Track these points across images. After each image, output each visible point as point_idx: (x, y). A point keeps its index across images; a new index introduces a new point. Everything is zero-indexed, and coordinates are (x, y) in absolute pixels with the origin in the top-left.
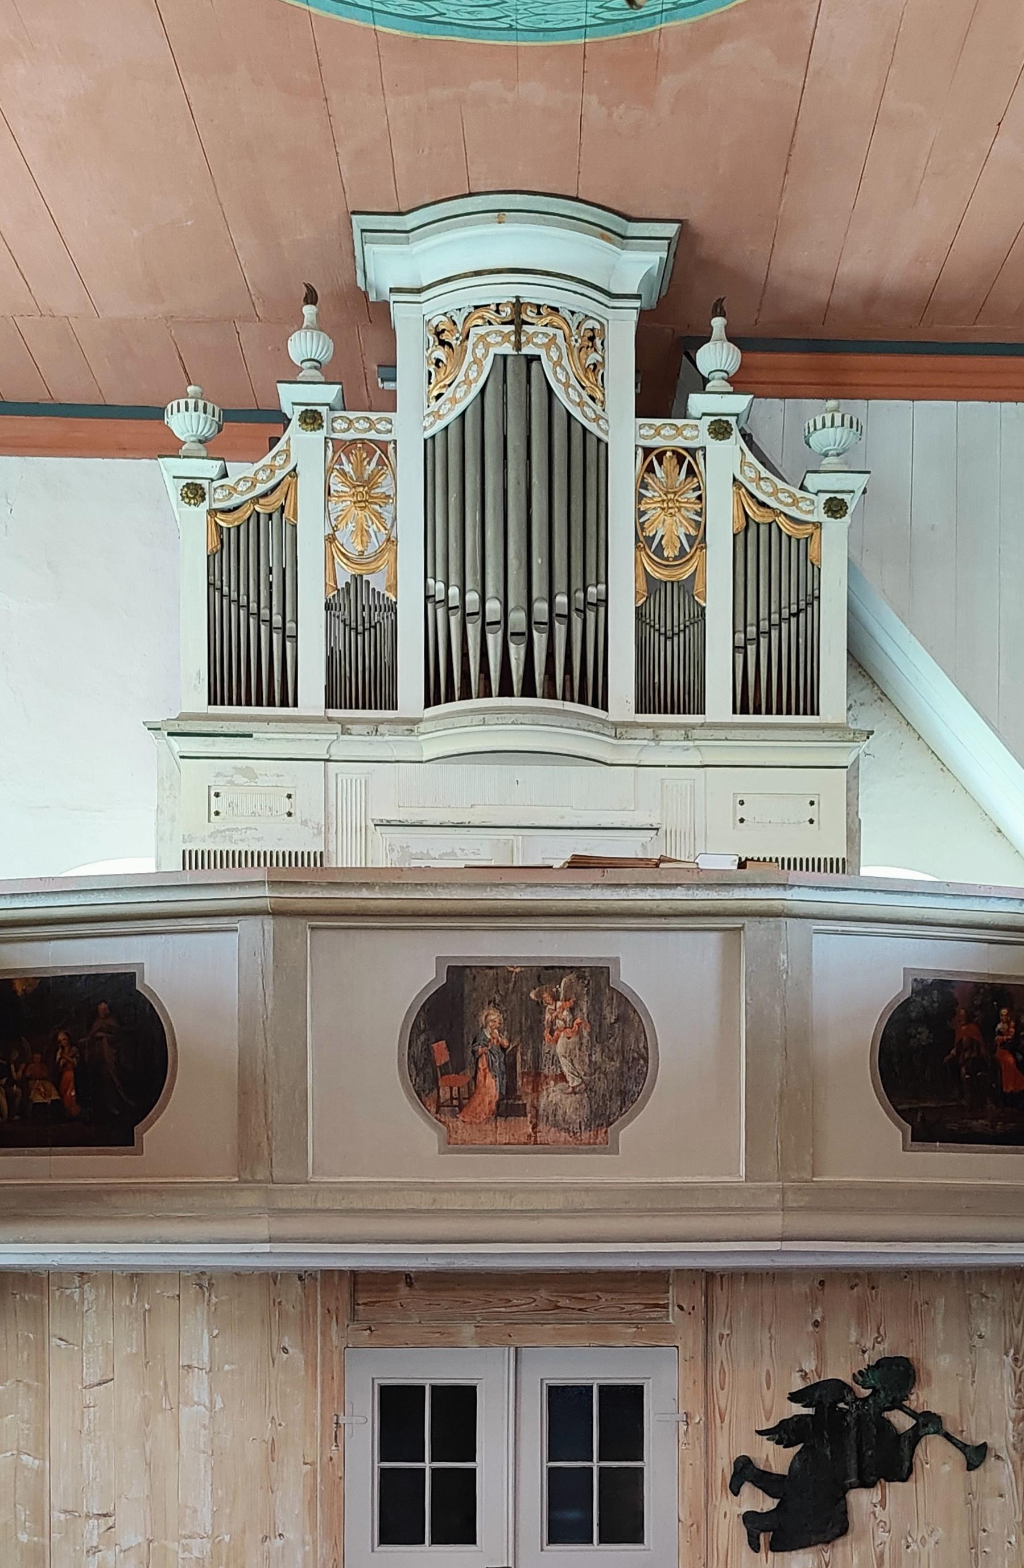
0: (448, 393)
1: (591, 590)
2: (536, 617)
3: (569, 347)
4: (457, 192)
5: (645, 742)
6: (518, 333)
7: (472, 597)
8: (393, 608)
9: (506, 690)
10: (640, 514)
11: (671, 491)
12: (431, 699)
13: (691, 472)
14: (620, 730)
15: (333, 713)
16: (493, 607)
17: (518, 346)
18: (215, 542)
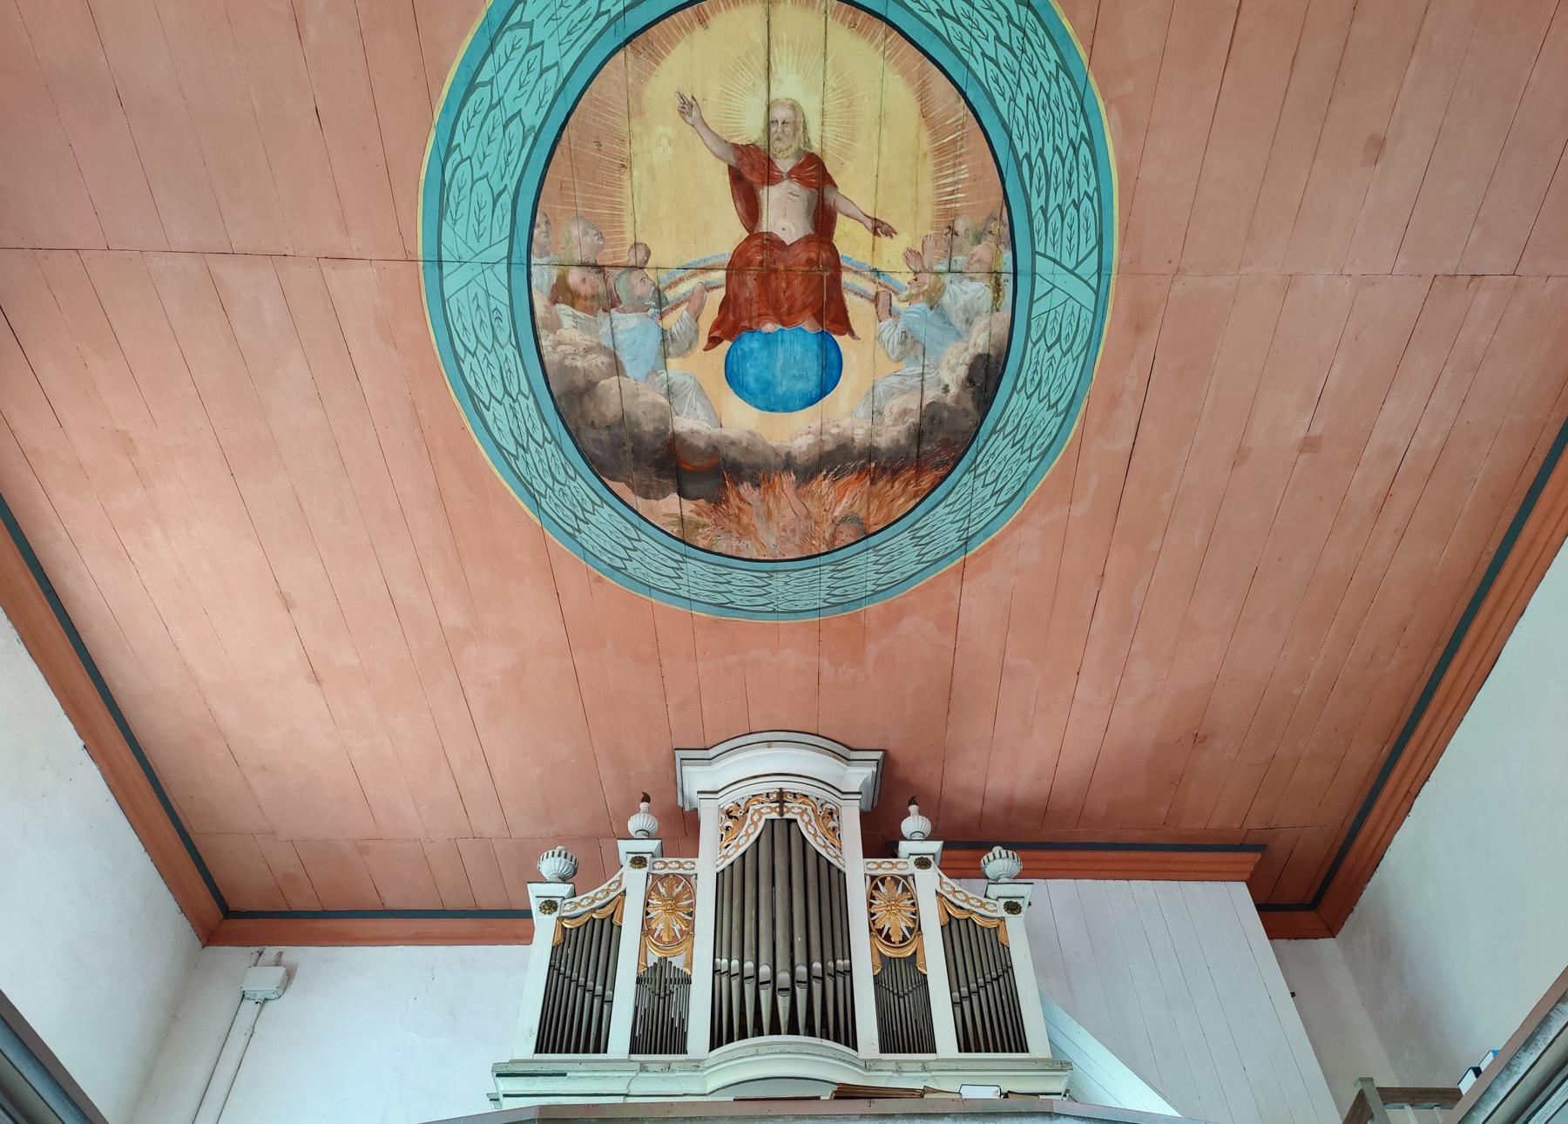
1: (839, 962)
2: (798, 978)
3: (817, 817)
6: (781, 807)
7: (749, 965)
9: (775, 1030)
10: (872, 915)
12: (715, 1043)
15: (634, 1057)
16: (765, 970)
17: (781, 814)
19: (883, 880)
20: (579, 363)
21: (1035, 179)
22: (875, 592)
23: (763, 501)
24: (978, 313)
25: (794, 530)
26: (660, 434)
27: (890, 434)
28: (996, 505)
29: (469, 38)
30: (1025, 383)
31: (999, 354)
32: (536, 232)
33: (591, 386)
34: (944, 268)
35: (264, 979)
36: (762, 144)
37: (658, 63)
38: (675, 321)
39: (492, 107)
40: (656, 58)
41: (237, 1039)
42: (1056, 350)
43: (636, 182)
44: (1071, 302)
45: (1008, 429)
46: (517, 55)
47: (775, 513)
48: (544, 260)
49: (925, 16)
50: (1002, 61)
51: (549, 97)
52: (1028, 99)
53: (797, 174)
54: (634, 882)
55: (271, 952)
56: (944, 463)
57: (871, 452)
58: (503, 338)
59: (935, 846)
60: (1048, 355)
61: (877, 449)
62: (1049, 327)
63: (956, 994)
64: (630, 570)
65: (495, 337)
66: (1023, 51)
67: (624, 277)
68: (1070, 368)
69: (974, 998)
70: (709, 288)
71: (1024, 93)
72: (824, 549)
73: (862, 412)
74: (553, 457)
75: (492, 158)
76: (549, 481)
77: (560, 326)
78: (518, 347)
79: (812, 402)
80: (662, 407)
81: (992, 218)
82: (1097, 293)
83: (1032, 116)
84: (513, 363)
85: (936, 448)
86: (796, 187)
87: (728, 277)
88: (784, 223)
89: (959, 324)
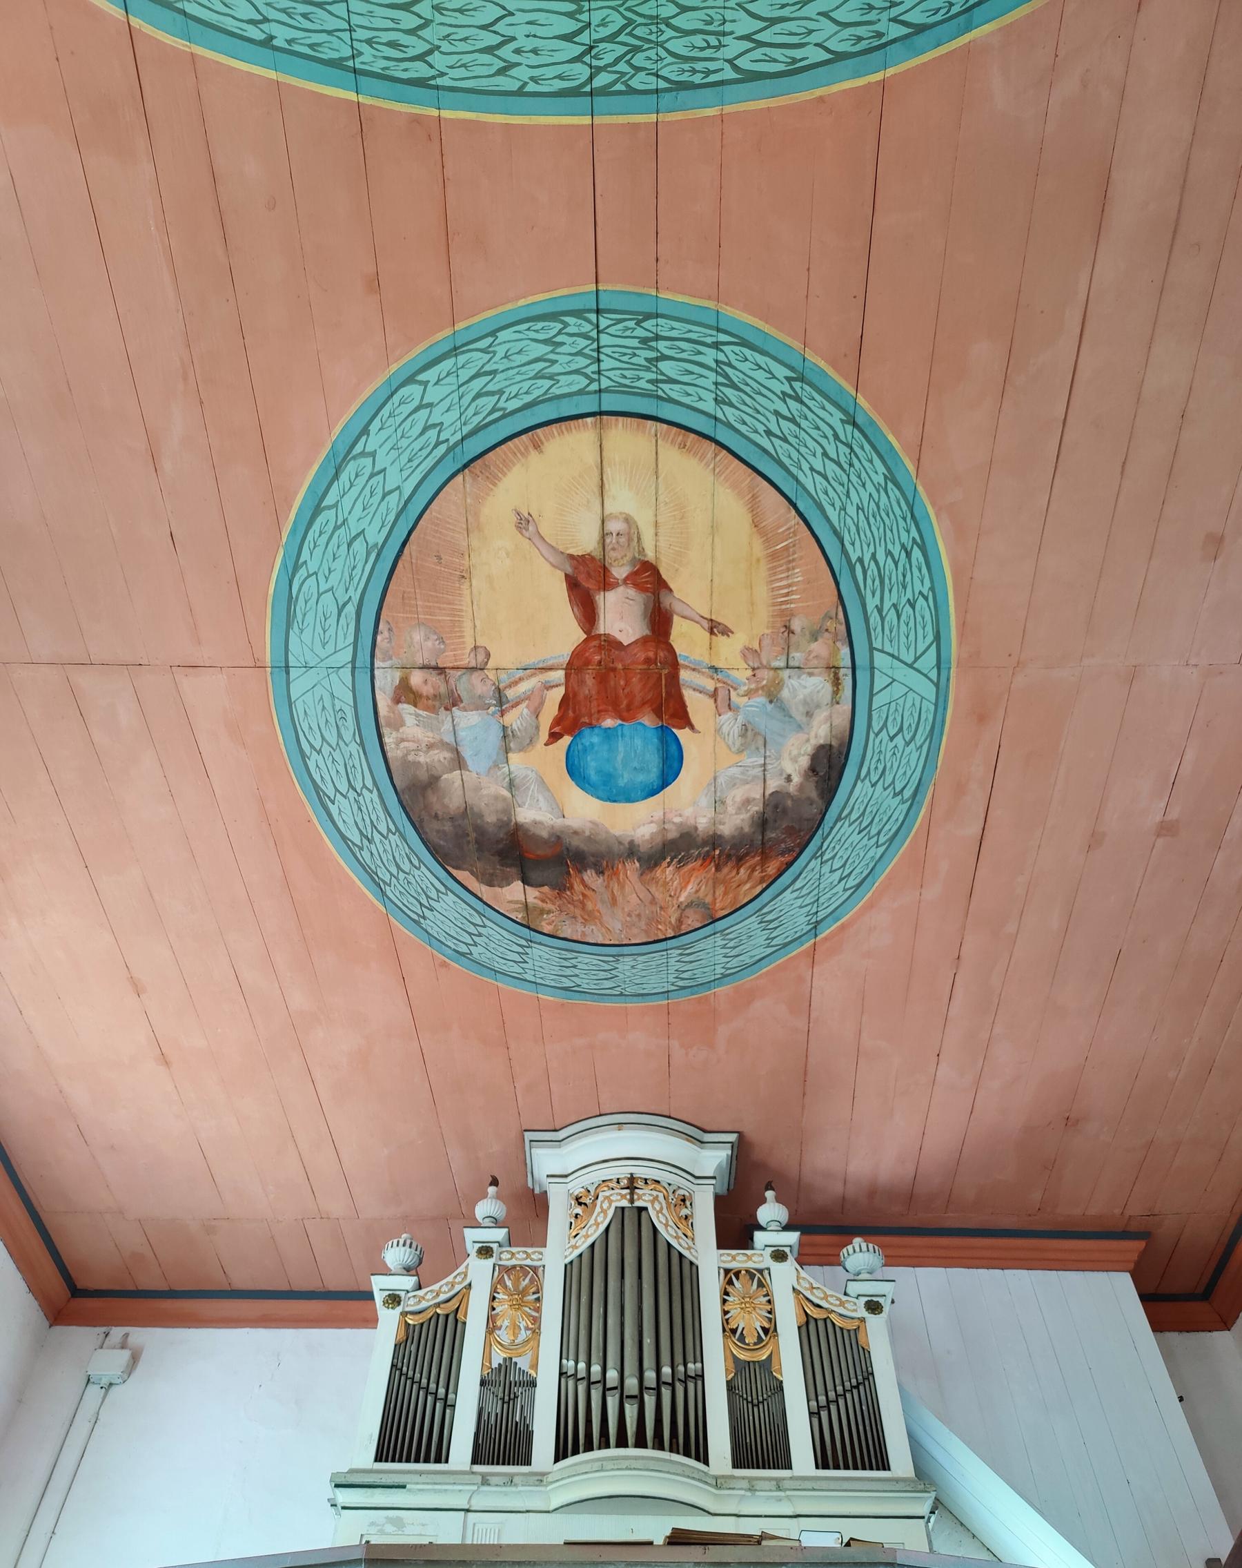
0: (583, 1232)
1: (690, 1366)
2: (647, 1383)
3: (668, 1204)
4: (594, 1114)
5: (742, 1492)
6: (632, 1194)
8: (533, 1384)
9: (622, 1442)
10: (726, 1313)
11: (747, 1299)
12: (561, 1453)
13: (761, 1285)
14: (719, 1482)
15: (477, 1468)
16: (612, 1375)
18: (402, 1334)
19: (737, 1274)
20: (422, 759)
21: (869, 581)
22: (724, 976)
23: (607, 887)
24: (818, 706)
25: (639, 916)
26: (503, 824)
27: (734, 822)
28: (845, 890)
29: (316, 467)
30: (868, 773)
31: (840, 745)
32: (379, 638)
33: (433, 781)
34: (782, 664)
35: (110, 1362)
36: (597, 554)
37: (495, 485)
38: (516, 718)
39: (336, 528)
40: (494, 480)
41: (82, 1426)
42: (899, 740)
43: (475, 591)
44: (911, 694)
45: (854, 817)
46: (361, 481)
47: (620, 899)
48: (388, 664)
49: (753, 436)
50: (830, 475)
51: (392, 517)
52: (858, 508)
53: (633, 580)
54: (479, 1272)
55: (117, 1332)
56: (790, 850)
57: (714, 840)
58: (347, 736)
59: (792, 1237)
60: (891, 745)
61: (720, 837)
62: (890, 719)
63: (813, 1403)
64: (476, 955)
65: (340, 736)
66: (851, 465)
67: (465, 678)
68: (913, 758)
69: (833, 1408)
70: (549, 687)
71: (856, 506)
72: (670, 933)
73: (705, 801)
74: (398, 848)
75: (337, 573)
76: (394, 870)
77: (402, 724)
78: (362, 744)
79: (653, 793)
80: (505, 799)
81: (828, 617)
82: (937, 685)
83: (863, 523)
84: (358, 760)
85: (781, 835)
86: (631, 592)
87: (567, 676)
88: (622, 625)
89: (799, 716)
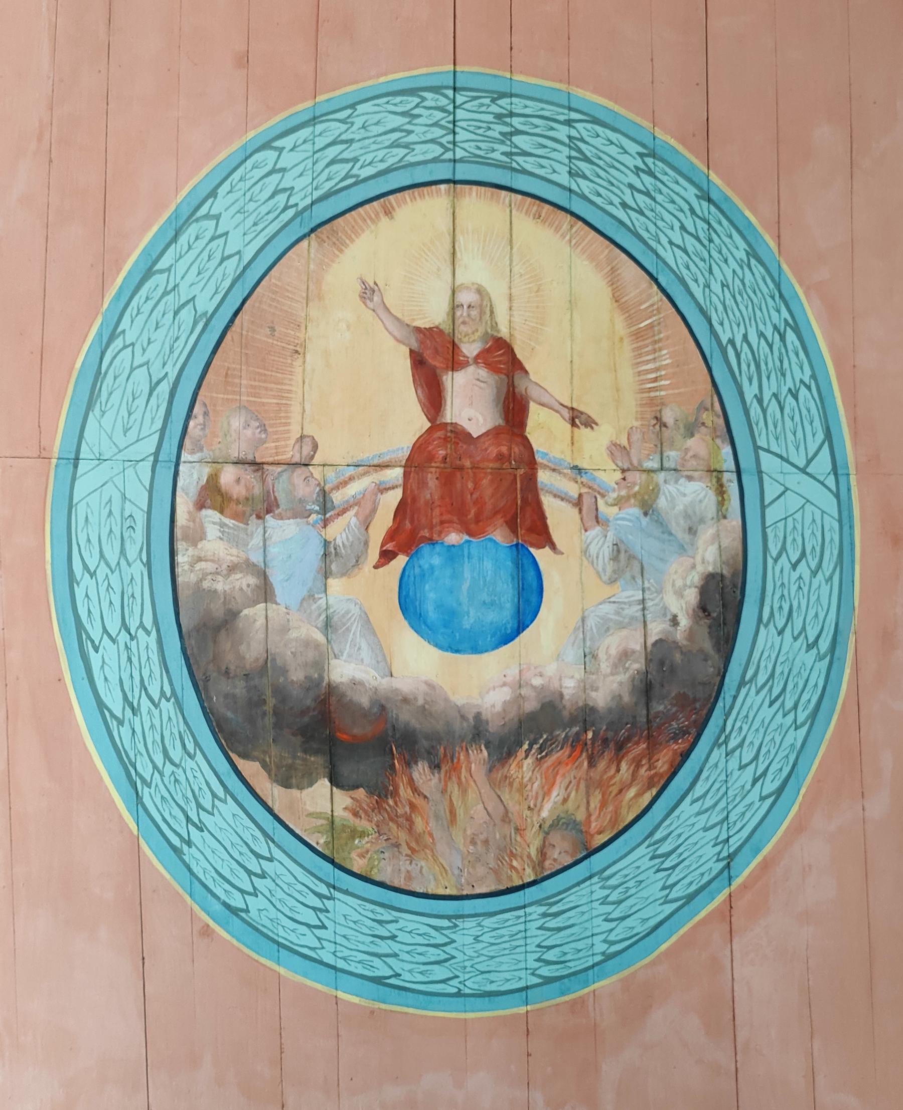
20: (220, 586)
23: (444, 791)
24: (702, 521)
26: (312, 684)
27: (609, 687)
28: (762, 799)
29: (155, 229)
30: (772, 614)
31: (734, 575)
32: (192, 424)
34: (655, 465)
36: (447, 328)
37: (341, 251)
38: (341, 530)
39: (166, 293)
40: (340, 246)
43: (308, 367)
45: (762, 678)
46: (201, 243)
47: (460, 812)
48: (196, 457)
51: (227, 284)
53: (483, 358)
56: (684, 732)
57: (586, 716)
58: (132, 552)
61: (593, 710)
65: (123, 552)
67: (285, 476)
68: (824, 592)
70: (383, 489)
72: (529, 876)
73: (572, 655)
75: (157, 343)
76: (159, 759)
77: (202, 536)
78: (148, 565)
79: (507, 639)
80: (317, 646)
84: (140, 589)
85: (667, 711)
86: (483, 373)
87: (406, 475)
88: (468, 412)
